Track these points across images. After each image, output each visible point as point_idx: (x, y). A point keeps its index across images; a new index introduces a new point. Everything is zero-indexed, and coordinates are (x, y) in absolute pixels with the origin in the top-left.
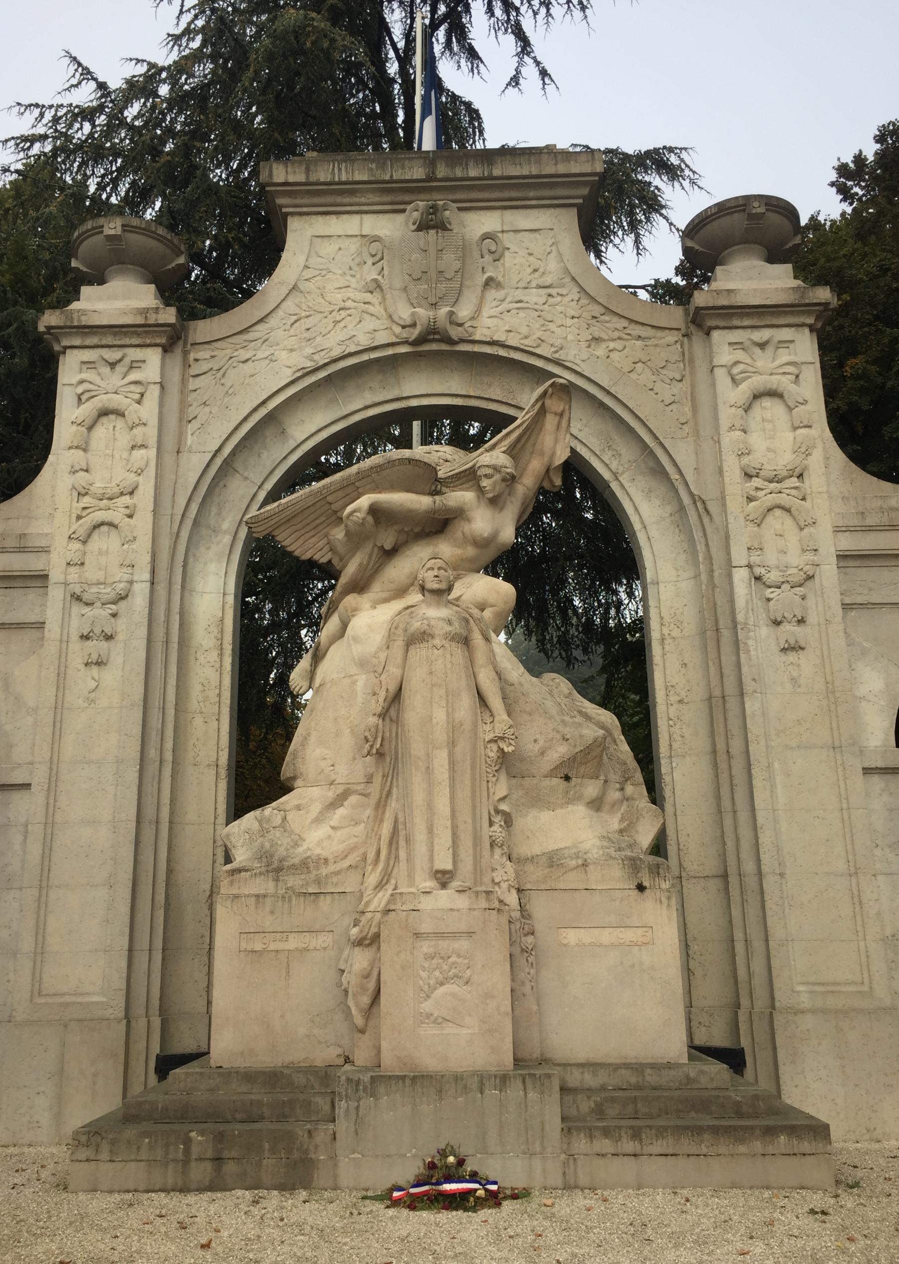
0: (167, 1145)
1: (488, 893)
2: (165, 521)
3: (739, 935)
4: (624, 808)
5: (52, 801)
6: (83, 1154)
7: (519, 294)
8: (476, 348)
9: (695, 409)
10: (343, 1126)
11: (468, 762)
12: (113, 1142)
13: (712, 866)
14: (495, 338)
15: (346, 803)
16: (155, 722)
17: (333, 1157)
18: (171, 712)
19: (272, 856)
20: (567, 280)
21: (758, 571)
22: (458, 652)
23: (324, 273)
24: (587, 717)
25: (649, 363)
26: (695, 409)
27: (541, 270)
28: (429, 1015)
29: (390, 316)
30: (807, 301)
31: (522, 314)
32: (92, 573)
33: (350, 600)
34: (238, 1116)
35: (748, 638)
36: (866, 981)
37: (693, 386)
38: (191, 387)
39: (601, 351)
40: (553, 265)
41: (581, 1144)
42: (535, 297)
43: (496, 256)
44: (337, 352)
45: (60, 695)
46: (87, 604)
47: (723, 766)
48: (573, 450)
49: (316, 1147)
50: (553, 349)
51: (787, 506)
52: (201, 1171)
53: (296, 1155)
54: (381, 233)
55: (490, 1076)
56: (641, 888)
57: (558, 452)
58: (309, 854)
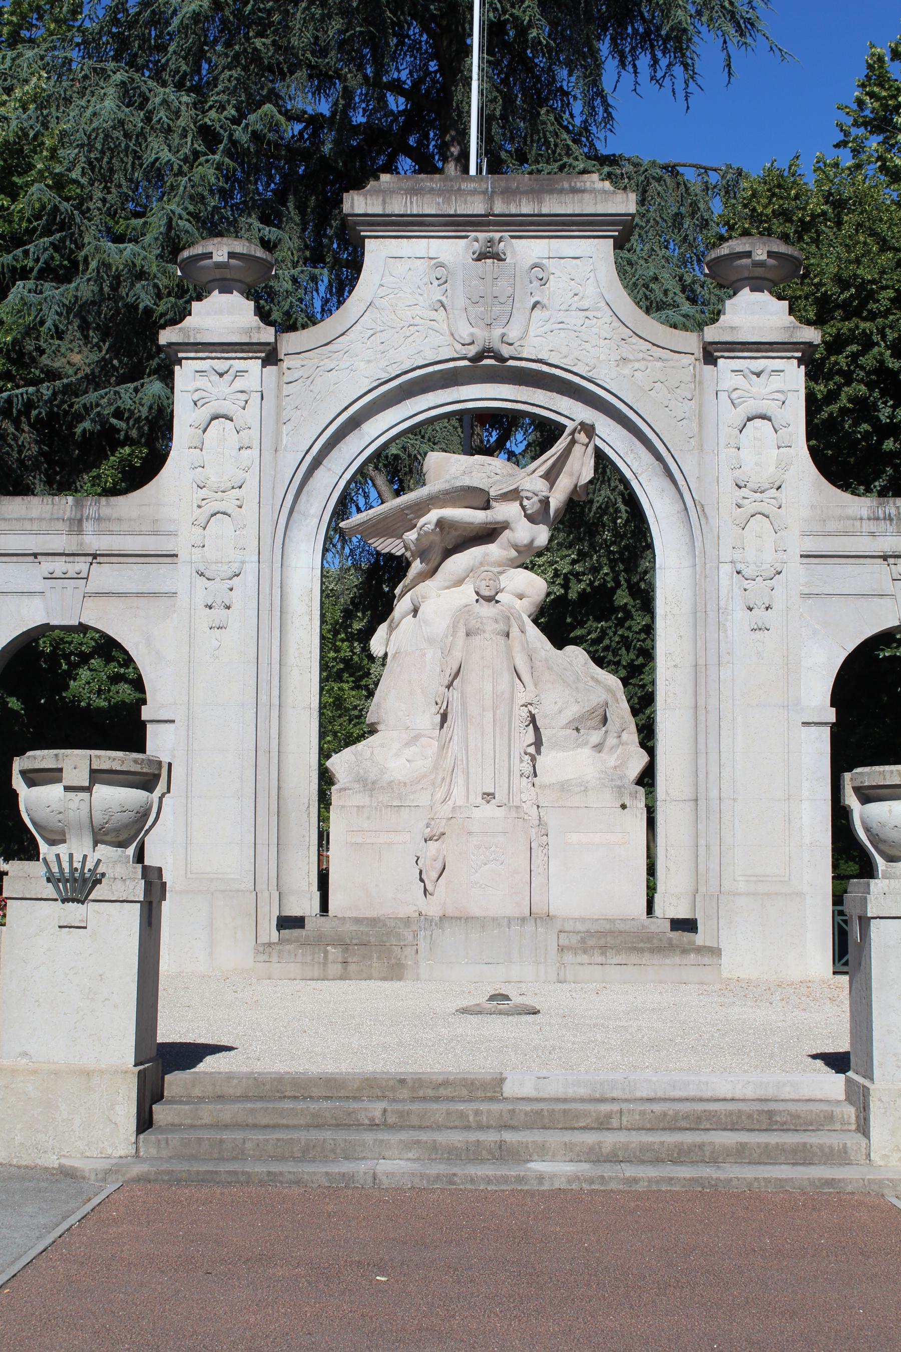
0: (313, 954)
1: (517, 807)
2: (266, 509)
3: (702, 842)
4: (619, 750)
5: (190, 734)
6: (262, 958)
7: (561, 316)
8: (524, 364)
9: (700, 425)
10: (423, 946)
11: (507, 720)
12: (280, 952)
13: (688, 793)
14: (540, 357)
15: (418, 743)
16: (263, 676)
17: (416, 963)
18: (276, 666)
19: (366, 780)
20: (603, 304)
21: (739, 567)
22: (502, 640)
23: (396, 291)
24: (597, 681)
25: (666, 383)
26: (700, 425)
27: (580, 295)
28: (476, 883)
29: (452, 335)
30: (795, 340)
31: (563, 334)
32: (211, 553)
33: (421, 588)
34: (354, 942)
35: (726, 620)
36: (787, 875)
37: (701, 406)
38: (285, 393)
39: (627, 371)
40: (590, 290)
41: (569, 957)
42: (575, 319)
43: (543, 282)
44: (407, 366)
45: (192, 652)
46: (208, 579)
47: (702, 718)
48: (600, 456)
49: (406, 957)
50: (588, 368)
51: (766, 513)
52: (335, 969)
53: (393, 961)
54: (444, 258)
55: (514, 918)
56: (624, 807)
57: (584, 474)
58: (392, 778)
